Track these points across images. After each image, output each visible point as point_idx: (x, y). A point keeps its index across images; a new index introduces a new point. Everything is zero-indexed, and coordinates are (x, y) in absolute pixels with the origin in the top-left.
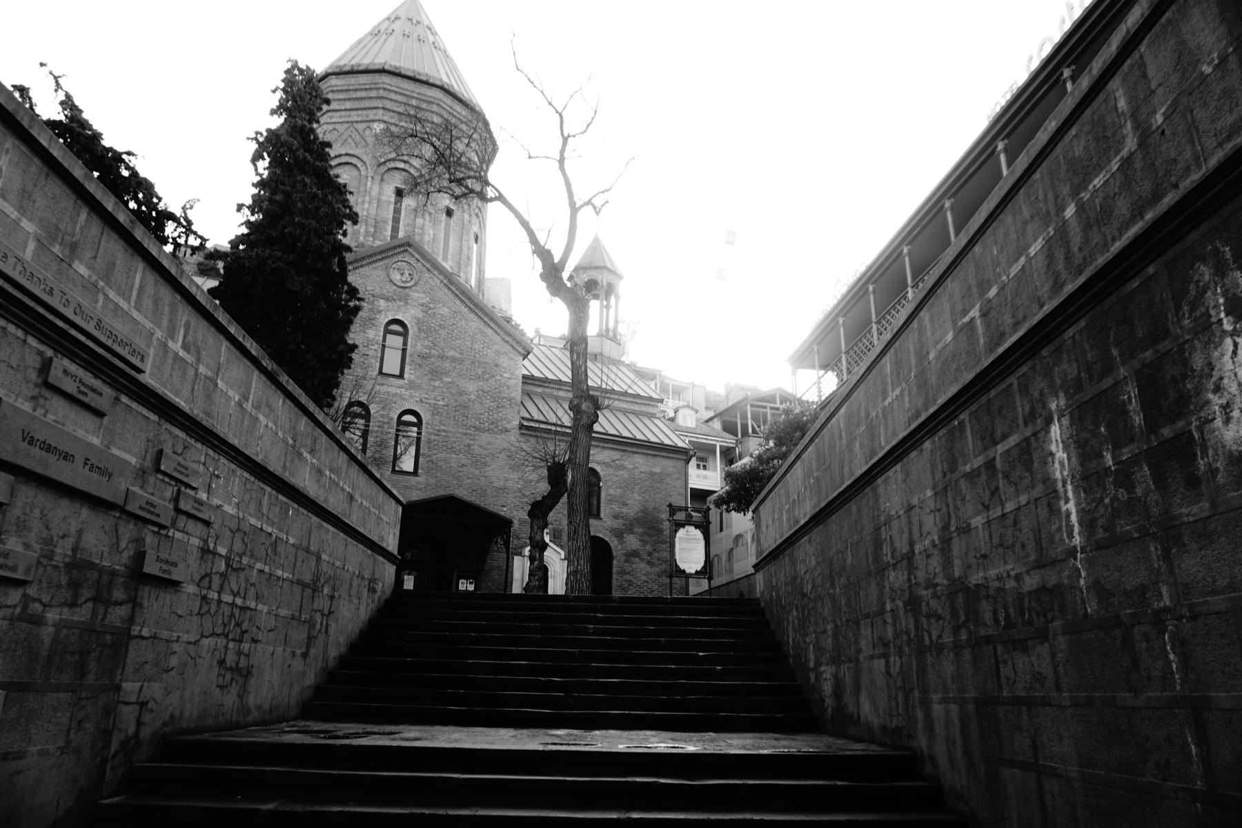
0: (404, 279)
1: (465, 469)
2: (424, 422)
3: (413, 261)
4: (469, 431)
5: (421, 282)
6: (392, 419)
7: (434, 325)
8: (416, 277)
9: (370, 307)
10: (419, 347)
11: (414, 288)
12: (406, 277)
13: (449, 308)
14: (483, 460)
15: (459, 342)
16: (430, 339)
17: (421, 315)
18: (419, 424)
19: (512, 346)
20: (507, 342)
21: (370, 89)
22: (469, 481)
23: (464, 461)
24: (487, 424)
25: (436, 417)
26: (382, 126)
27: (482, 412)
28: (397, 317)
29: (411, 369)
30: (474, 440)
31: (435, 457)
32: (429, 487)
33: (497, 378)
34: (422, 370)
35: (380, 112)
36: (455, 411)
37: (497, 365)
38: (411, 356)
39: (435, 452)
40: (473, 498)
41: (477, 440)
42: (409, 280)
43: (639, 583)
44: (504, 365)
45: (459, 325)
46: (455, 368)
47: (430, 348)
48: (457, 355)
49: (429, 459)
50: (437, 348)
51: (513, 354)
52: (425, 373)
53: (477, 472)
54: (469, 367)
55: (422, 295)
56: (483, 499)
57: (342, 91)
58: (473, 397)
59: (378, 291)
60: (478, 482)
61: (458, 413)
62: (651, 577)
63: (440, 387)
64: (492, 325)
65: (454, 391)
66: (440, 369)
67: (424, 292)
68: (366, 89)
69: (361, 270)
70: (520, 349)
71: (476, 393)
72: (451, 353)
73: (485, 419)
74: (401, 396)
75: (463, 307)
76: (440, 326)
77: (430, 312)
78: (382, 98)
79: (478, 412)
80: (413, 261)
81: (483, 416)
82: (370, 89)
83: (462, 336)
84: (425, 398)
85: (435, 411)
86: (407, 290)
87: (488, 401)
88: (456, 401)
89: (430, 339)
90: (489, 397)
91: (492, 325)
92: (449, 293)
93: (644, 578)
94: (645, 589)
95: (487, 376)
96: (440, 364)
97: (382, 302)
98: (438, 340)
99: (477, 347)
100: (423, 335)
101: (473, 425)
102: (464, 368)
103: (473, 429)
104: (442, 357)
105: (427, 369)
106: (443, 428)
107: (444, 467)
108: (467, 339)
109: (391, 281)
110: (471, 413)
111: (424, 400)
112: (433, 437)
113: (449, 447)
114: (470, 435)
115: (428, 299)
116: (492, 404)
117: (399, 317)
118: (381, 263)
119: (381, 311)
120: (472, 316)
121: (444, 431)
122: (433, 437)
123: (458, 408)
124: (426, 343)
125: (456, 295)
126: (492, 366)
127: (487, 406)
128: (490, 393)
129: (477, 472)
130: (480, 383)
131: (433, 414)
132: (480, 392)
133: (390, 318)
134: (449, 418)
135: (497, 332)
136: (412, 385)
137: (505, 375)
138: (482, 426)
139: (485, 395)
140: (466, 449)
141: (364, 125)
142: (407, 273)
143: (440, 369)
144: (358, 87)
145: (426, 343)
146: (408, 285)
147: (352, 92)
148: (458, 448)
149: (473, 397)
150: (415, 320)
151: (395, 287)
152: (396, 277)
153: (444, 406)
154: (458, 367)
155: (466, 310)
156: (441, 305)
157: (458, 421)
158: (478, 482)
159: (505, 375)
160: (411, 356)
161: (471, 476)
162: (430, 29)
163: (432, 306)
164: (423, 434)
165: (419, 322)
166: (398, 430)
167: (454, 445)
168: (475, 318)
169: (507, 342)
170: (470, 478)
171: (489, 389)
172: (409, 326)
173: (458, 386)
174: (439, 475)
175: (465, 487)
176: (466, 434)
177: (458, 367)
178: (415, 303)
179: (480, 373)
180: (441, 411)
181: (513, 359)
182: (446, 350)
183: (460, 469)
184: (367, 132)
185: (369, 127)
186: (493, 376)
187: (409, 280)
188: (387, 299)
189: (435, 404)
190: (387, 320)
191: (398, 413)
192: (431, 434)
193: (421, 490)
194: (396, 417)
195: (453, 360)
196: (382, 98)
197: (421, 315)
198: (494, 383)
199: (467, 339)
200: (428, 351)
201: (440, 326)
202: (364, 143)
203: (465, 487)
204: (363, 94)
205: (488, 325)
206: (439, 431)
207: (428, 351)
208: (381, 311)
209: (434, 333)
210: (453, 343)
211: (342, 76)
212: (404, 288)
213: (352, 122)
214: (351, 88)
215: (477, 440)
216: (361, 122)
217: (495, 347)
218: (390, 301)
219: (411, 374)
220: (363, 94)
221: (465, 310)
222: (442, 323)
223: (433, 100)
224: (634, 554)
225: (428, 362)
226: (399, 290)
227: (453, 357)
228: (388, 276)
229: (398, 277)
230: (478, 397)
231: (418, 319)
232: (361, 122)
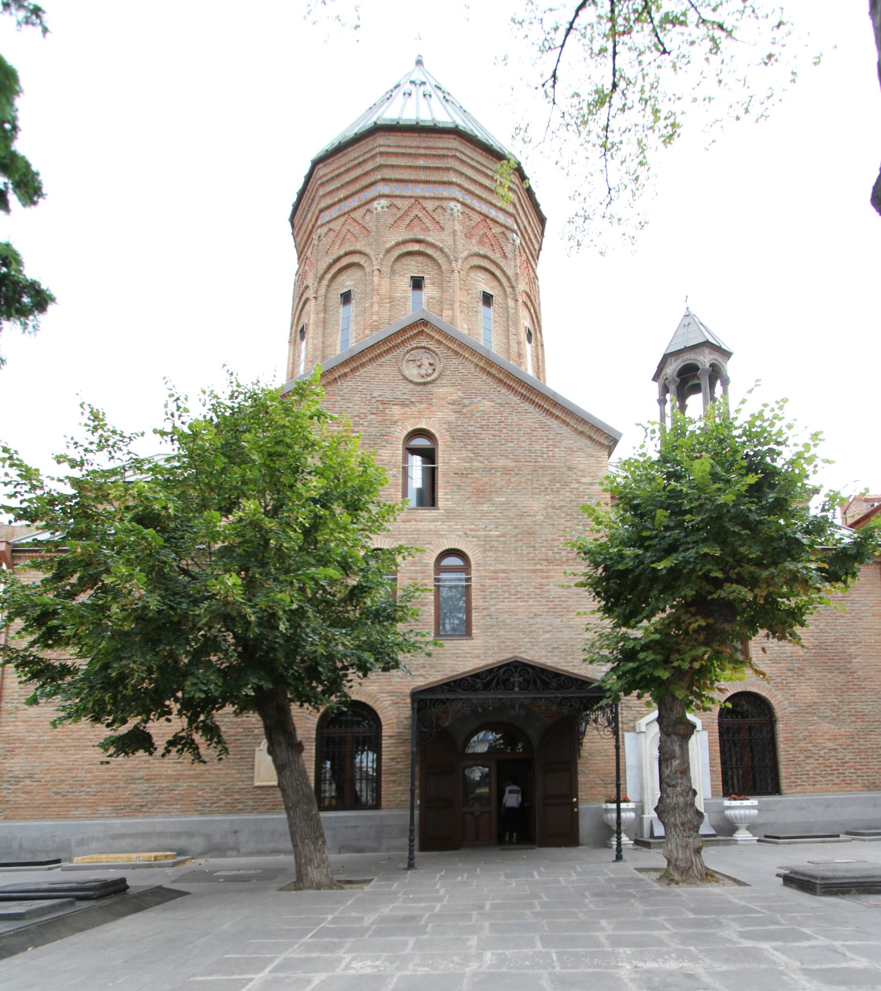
0: (423, 372)
1: (538, 619)
2: (472, 563)
3: (433, 346)
4: (539, 567)
5: (448, 372)
6: (427, 565)
7: (470, 428)
8: (439, 368)
9: (380, 419)
10: (455, 461)
11: (439, 381)
12: (426, 369)
13: (492, 400)
14: (565, 605)
15: (510, 444)
16: (470, 448)
17: (453, 418)
18: (466, 568)
19: (590, 437)
20: (581, 433)
21: (365, 161)
22: (548, 636)
23: (536, 609)
24: (564, 553)
25: (489, 554)
26: (384, 202)
27: (556, 537)
28: (419, 426)
29: (447, 494)
30: (547, 577)
31: (493, 609)
32: (490, 652)
33: (572, 486)
34: (463, 492)
35: (381, 185)
36: (516, 541)
37: (570, 468)
38: (444, 475)
39: (493, 602)
40: (556, 659)
41: (553, 577)
42: (430, 371)
43: (822, 753)
44: (581, 467)
45: (509, 421)
46: (509, 482)
47: (471, 460)
48: (511, 464)
49: (485, 612)
50: (481, 459)
51: (591, 449)
52: (468, 495)
53: (557, 622)
54: (530, 477)
55: (450, 390)
56: (569, 658)
57: (332, 179)
58: (540, 518)
59: (388, 395)
60: (560, 635)
61: (520, 543)
62: (840, 741)
63: (491, 512)
64: (557, 413)
65: (512, 515)
66: (487, 486)
67: (454, 385)
68: (360, 164)
69: (362, 370)
70: (602, 440)
71: (544, 512)
72: (502, 462)
73: (561, 547)
74: (436, 533)
75: (511, 396)
76: (482, 427)
77: (465, 411)
78: (380, 167)
79: (550, 537)
80: (433, 346)
81: (557, 543)
82: (365, 161)
83: (515, 436)
84: (471, 530)
85: (487, 545)
86: (429, 386)
87: (562, 521)
88: (516, 527)
89: (470, 448)
90: (563, 515)
91: (557, 413)
92: (489, 380)
93: (830, 745)
94: (832, 760)
95: (558, 485)
96: (487, 479)
97: (396, 410)
98: (480, 447)
99: (538, 447)
100: (458, 444)
101: (543, 556)
102: (523, 480)
103: (545, 563)
104: (490, 470)
105: (469, 489)
106: (500, 567)
107: (508, 621)
108: (522, 439)
109: (405, 378)
110: (539, 540)
111: (469, 533)
112: (488, 582)
113: (513, 591)
114: (541, 571)
115: (460, 393)
116: (569, 524)
117: (423, 425)
118: (388, 357)
119: (396, 422)
120: (526, 406)
121: (503, 571)
122: (488, 582)
123: (520, 537)
124: (464, 454)
125: (500, 381)
126: (564, 470)
127: (562, 527)
128: (564, 509)
129: (557, 622)
130: (548, 497)
131: (485, 551)
132: (550, 510)
133: (410, 429)
134: (509, 553)
135: (564, 422)
136: (451, 515)
137: (584, 480)
138: (557, 556)
139: (557, 512)
140: (538, 591)
141: (362, 211)
142: (426, 362)
143: (487, 486)
144: (350, 165)
145: (464, 454)
146: (429, 379)
147: (344, 176)
148: (526, 592)
149: (540, 518)
150: (445, 426)
151: (412, 386)
152: (412, 372)
153: (499, 536)
154: (513, 480)
155: (516, 399)
156: (479, 398)
157: (521, 555)
158: (560, 635)
159: (584, 480)
160: (444, 475)
161: (550, 628)
162: (440, 89)
163: (466, 402)
164: (473, 579)
165: (451, 427)
166: (437, 580)
167: (519, 589)
168: (531, 408)
169: (581, 433)
170: (547, 632)
171: (562, 503)
172: (437, 435)
173: (515, 506)
174: (502, 632)
175: (542, 644)
176: (535, 571)
177: (513, 480)
178: (442, 402)
179: (546, 483)
180: (496, 544)
181: (593, 456)
182: (494, 459)
183: (531, 621)
184: (368, 217)
185: (369, 210)
186: (566, 484)
187: (430, 371)
188: (403, 405)
189: (486, 536)
190: (405, 433)
191: (435, 555)
192: (483, 578)
193: (478, 657)
194: (432, 562)
195: (506, 471)
196: (380, 167)
197: (453, 418)
198: (568, 494)
199: (522, 439)
200: (467, 465)
201: (482, 427)
202: (365, 232)
203: (542, 644)
204: (359, 172)
205: (552, 414)
206: (496, 572)
207: (467, 465)
208: (396, 422)
209: (474, 439)
210: (503, 448)
211: (330, 161)
212: (425, 384)
213: (349, 212)
214: (343, 169)
215: (553, 577)
216: (359, 207)
217: (565, 443)
218: (407, 405)
219: (447, 500)
220: (359, 172)
221: (516, 399)
222: (484, 423)
223: (445, 152)
224: (810, 709)
225: (469, 481)
226: (419, 388)
227: (504, 468)
228: (400, 372)
229: (415, 371)
230: (548, 517)
231: (449, 423)
232: (359, 207)
